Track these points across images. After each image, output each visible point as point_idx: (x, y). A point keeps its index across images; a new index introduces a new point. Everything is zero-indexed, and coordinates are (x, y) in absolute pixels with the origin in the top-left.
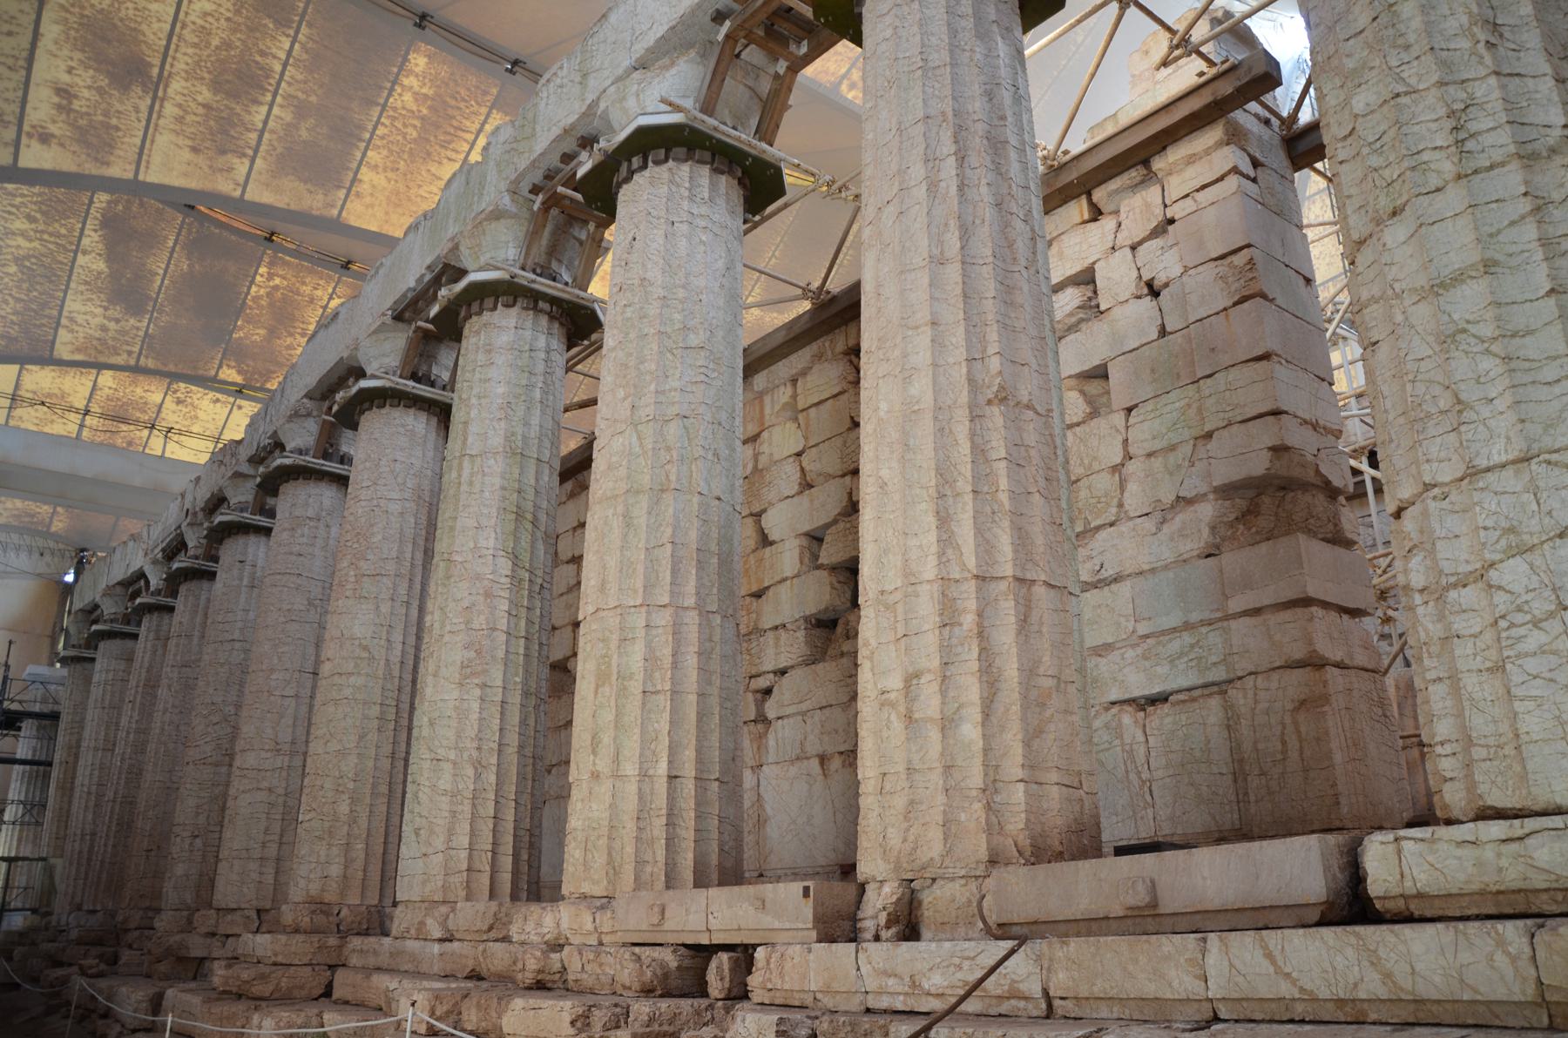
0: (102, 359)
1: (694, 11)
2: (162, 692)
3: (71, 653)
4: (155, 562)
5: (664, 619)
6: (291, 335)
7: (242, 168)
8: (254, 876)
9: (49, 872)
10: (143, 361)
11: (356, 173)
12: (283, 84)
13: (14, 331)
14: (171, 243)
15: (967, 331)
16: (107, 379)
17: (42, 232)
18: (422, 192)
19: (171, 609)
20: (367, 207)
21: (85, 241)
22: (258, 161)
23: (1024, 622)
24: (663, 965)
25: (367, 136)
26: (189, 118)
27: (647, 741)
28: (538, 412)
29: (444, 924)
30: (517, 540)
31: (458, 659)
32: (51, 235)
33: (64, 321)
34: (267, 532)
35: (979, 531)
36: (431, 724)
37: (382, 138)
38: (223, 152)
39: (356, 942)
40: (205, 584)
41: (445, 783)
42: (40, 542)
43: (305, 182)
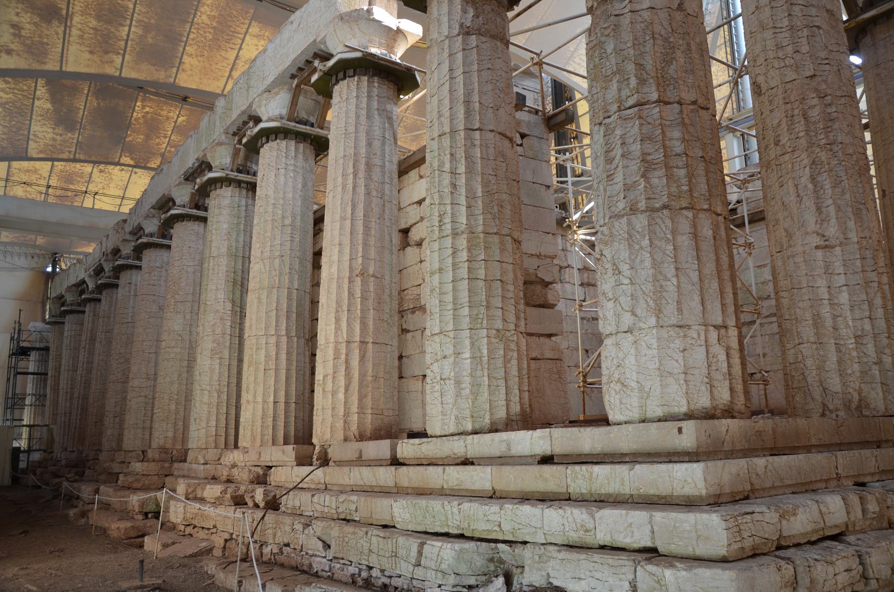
0: (55, 156)
1: (285, 71)
2: (97, 345)
3: (53, 320)
4: (90, 276)
5: (273, 340)
6: (158, 137)
7: (118, 60)
8: (140, 436)
9: (50, 431)
10: (77, 156)
11: (181, 59)
12: (135, 15)
13: (5, 144)
14: (86, 92)
15: (351, 248)
16: (59, 165)
17: (13, 89)
18: (218, 66)
19: (99, 300)
20: (189, 76)
21: (38, 93)
22: (127, 56)
23: (362, 358)
24: (258, 473)
25: (185, 39)
26: (86, 36)
27: (266, 388)
28: (242, 235)
29: (204, 458)
30: (234, 294)
31: (210, 347)
32: (18, 90)
33: (31, 137)
34: (139, 268)
35: (349, 324)
36: (200, 374)
37: (193, 40)
38: (107, 53)
39: (176, 465)
40: (115, 291)
41: (206, 399)
42: (32, 251)
43: (154, 65)
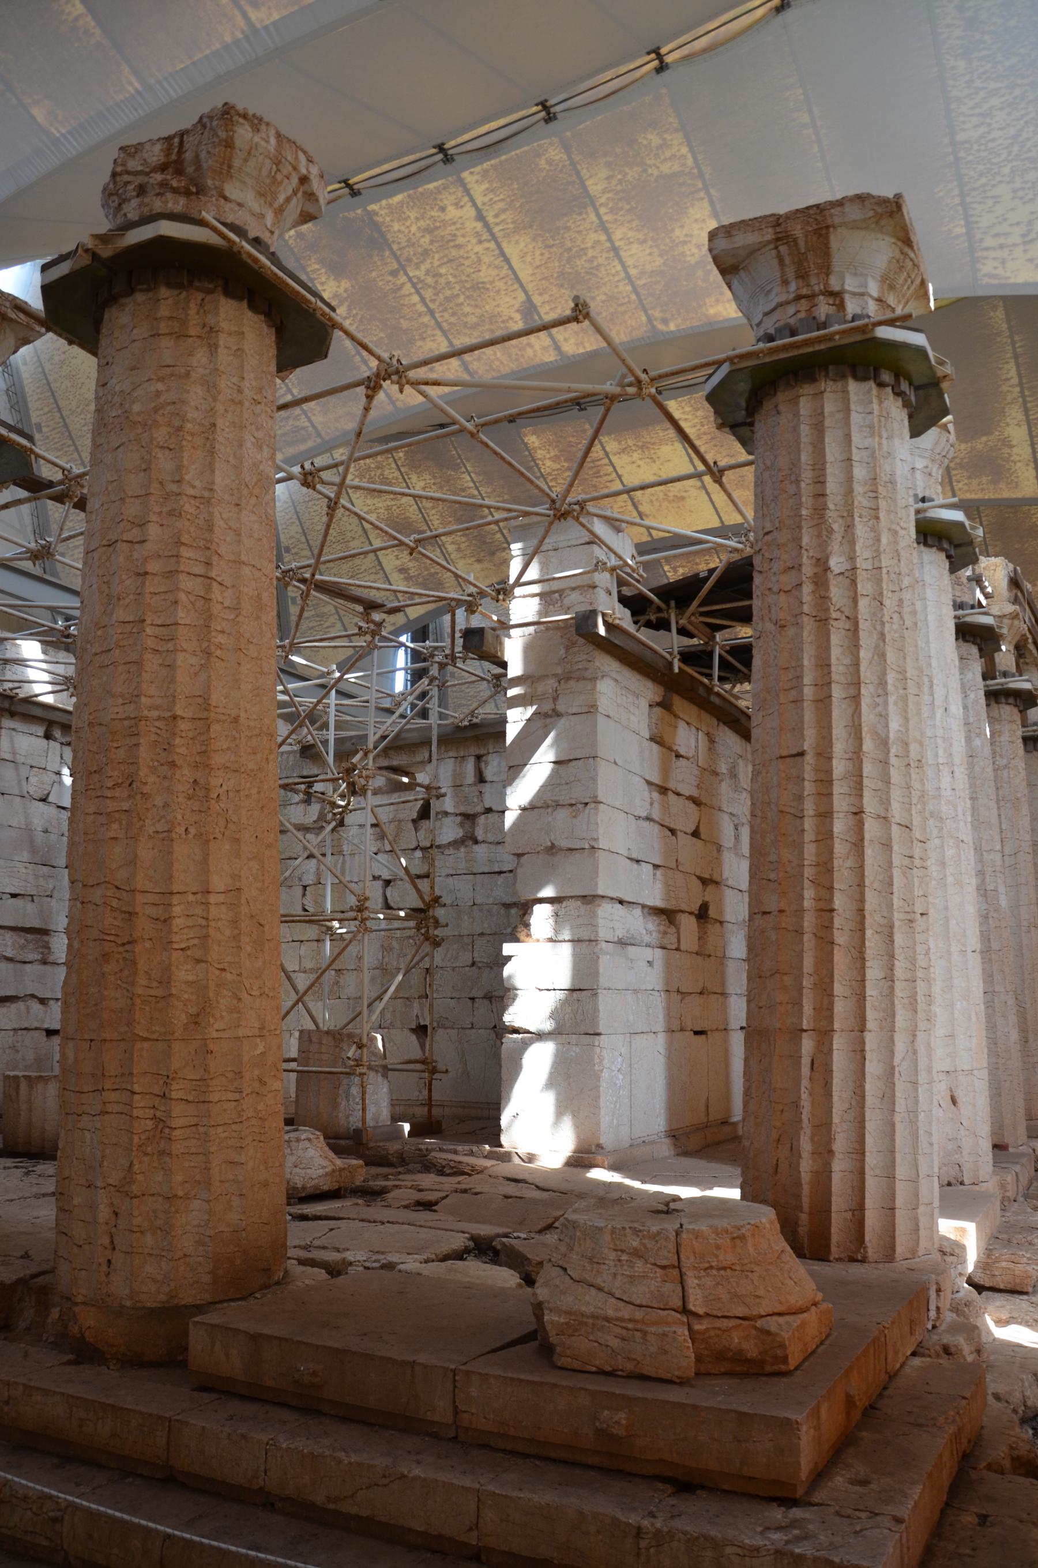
26: (463, 546)
38: (493, 554)
